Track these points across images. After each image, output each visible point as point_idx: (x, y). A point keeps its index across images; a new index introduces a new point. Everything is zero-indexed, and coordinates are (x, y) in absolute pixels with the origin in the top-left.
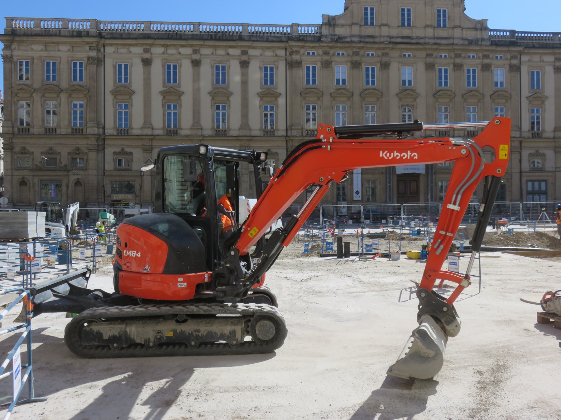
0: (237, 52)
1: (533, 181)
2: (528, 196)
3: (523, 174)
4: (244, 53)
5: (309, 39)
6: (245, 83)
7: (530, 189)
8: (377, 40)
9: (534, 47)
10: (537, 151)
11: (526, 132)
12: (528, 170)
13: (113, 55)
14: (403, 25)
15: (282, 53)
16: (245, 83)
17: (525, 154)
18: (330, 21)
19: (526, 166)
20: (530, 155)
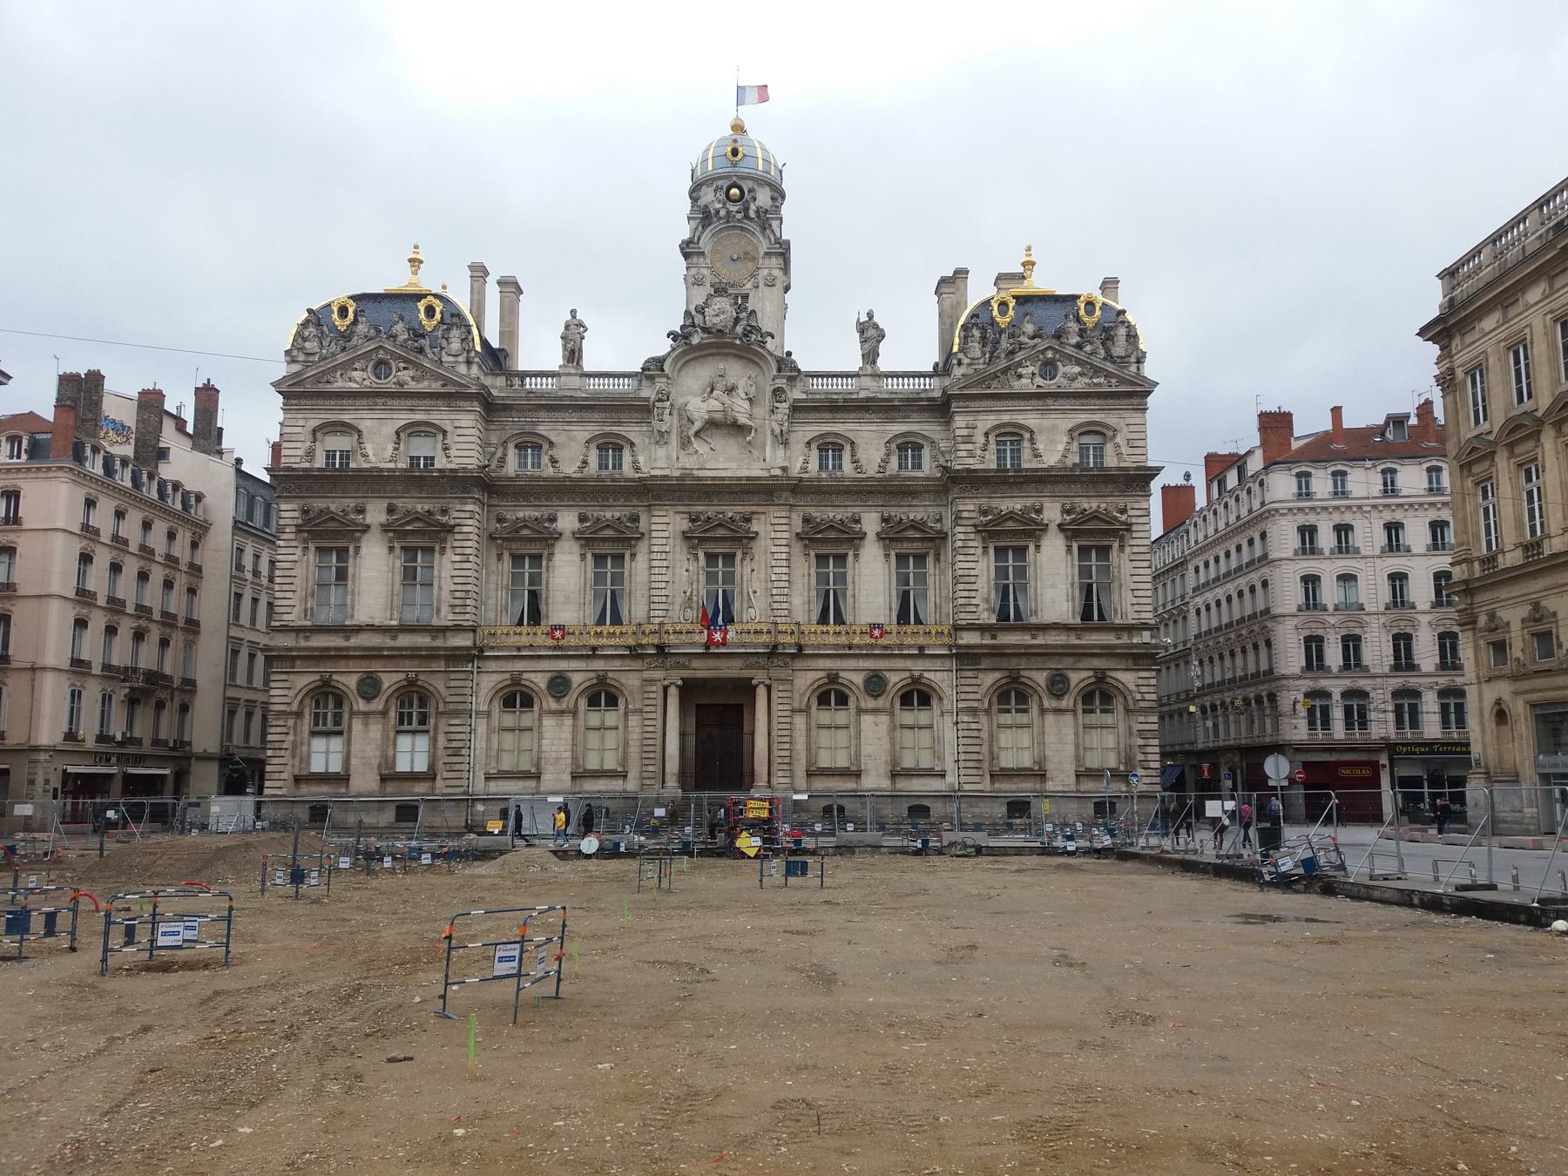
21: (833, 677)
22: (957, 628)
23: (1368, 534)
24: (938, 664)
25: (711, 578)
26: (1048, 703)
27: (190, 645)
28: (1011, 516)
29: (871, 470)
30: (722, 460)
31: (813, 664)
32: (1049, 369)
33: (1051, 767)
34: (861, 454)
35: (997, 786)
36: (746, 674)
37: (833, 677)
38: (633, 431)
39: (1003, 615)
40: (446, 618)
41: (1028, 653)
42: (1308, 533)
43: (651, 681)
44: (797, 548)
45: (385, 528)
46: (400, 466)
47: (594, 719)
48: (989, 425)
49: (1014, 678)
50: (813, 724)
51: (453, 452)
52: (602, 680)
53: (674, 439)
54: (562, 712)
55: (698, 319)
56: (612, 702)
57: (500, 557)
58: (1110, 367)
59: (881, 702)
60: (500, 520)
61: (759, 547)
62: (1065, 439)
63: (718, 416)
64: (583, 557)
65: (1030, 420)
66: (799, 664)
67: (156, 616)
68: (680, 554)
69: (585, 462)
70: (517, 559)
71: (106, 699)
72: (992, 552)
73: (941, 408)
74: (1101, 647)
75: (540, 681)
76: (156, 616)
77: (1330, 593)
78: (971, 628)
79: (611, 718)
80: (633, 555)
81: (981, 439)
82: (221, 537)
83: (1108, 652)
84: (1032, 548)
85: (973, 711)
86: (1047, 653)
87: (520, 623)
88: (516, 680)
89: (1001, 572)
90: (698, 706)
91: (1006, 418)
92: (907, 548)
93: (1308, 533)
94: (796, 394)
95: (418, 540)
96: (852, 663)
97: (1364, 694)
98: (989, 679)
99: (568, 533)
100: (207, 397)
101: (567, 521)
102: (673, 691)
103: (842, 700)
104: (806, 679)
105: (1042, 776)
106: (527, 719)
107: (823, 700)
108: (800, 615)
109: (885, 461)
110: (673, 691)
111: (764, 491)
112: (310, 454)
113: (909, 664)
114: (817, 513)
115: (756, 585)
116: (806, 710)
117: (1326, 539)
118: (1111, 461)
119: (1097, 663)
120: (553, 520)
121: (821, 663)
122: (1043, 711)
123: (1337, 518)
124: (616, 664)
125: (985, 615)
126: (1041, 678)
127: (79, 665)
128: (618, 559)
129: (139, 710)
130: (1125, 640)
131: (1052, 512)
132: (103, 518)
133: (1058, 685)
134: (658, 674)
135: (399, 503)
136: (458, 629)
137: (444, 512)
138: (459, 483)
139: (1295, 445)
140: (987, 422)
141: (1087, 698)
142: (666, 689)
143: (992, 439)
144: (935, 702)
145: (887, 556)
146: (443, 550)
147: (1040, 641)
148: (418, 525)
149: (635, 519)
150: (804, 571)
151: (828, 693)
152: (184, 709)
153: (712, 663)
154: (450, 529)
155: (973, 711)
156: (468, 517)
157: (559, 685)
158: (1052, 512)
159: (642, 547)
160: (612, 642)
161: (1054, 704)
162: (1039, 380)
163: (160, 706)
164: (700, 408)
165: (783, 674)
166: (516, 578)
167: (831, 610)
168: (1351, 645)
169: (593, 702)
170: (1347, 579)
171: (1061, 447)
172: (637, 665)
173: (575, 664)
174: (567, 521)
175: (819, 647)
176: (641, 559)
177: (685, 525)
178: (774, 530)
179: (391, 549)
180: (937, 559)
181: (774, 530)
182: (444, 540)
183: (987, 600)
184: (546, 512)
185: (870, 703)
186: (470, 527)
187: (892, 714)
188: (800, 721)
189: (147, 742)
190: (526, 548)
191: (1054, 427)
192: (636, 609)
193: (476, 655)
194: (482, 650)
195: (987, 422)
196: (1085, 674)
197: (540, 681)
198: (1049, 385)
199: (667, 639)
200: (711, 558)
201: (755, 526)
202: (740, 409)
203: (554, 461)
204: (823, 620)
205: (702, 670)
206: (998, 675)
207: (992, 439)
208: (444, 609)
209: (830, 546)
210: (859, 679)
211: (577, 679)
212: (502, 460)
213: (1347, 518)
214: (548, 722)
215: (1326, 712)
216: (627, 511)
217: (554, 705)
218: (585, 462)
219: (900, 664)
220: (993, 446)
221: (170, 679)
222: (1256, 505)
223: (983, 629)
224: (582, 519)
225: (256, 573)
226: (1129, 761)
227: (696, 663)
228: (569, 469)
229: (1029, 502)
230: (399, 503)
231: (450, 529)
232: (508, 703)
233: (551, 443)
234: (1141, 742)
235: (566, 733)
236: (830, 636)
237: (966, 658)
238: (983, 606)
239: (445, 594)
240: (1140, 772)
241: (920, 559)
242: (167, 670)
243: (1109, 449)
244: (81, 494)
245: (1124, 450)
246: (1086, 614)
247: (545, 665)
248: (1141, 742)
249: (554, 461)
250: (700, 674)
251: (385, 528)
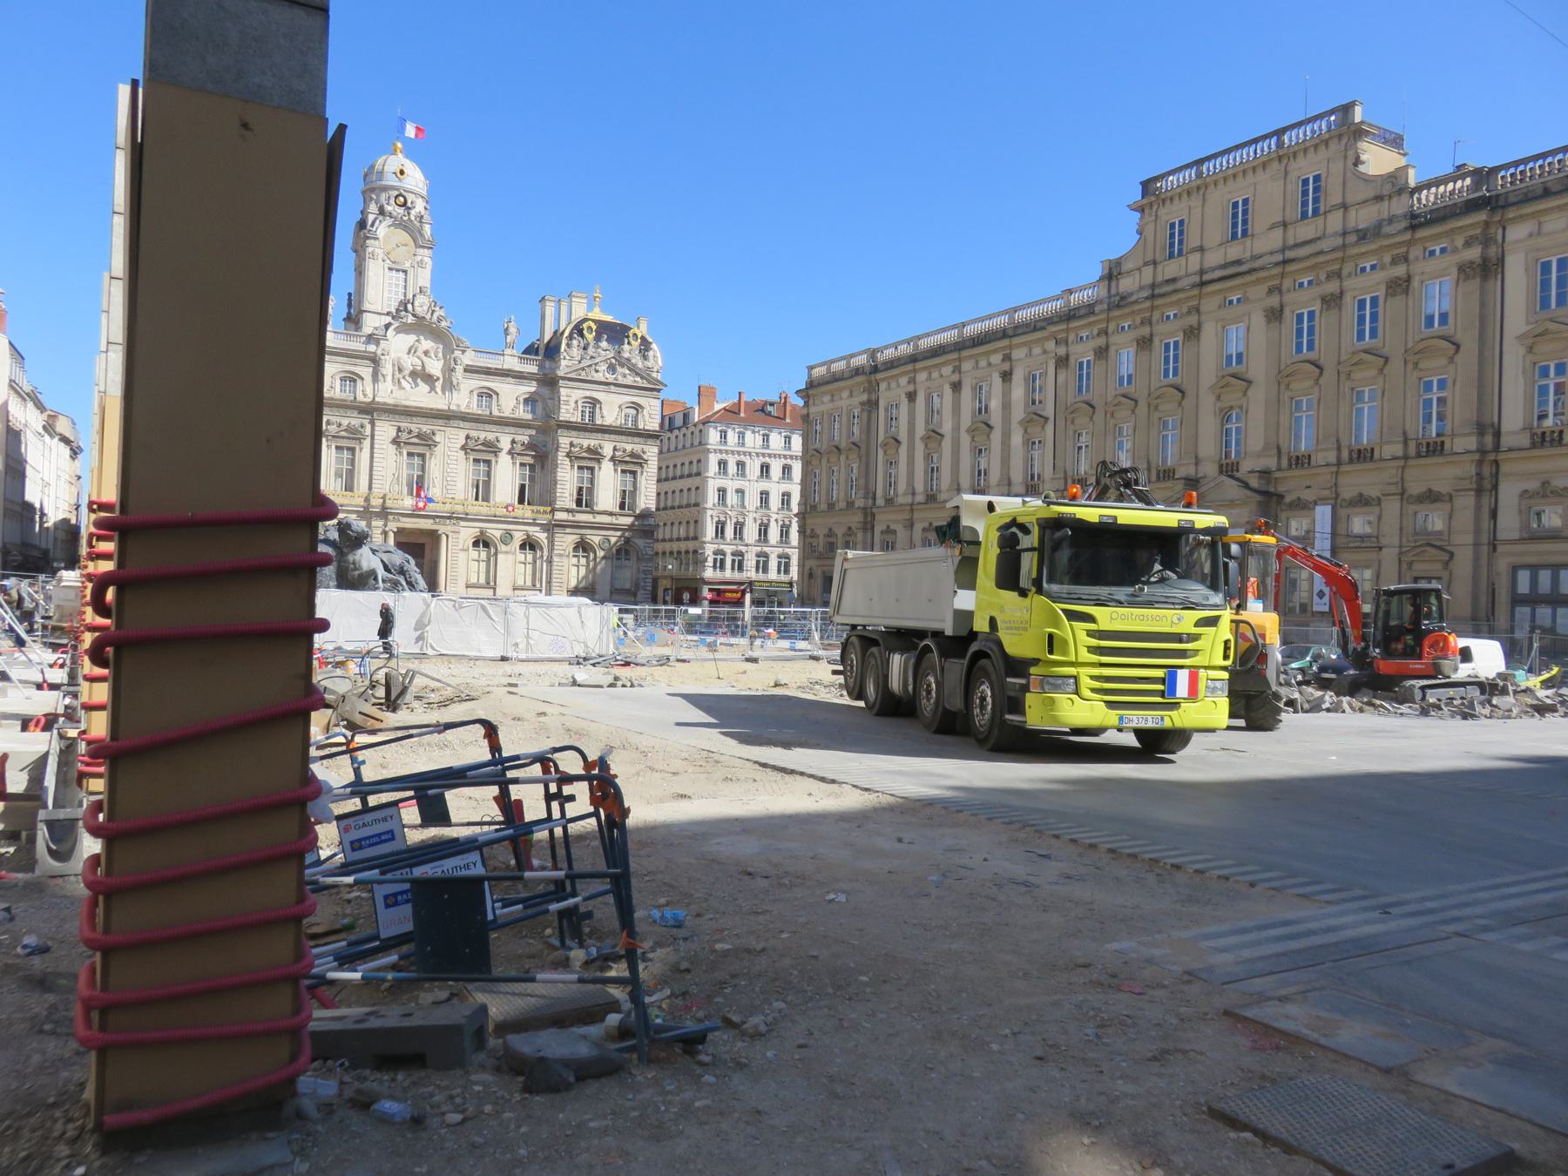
0: (996, 359)
1: (1534, 569)
2: (1518, 609)
3: (1500, 548)
4: (1007, 358)
5: (1082, 312)
6: (1006, 406)
7: (1523, 587)
8: (1179, 285)
9: (1547, 193)
10: (1545, 483)
11: (1514, 433)
12: (1516, 535)
13: (892, 392)
14: (1234, 236)
15: (1051, 345)
16: (1006, 406)
17: (1509, 493)
18: (1112, 273)
19: (1509, 524)
20: (1524, 494)
23: (753, 468)
28: (589, 450)
29: (507, 413)
30: (419, 396)
32: (612, 368)
38: (366, 371)
42: (723, 464)
53: (389, 378)
55: (410, 307)
61: (438, 450)
77: (732, 498)
91: (588, 394)
93: (723, 464)
94: (469, 358)
97: (741, 554)
108: (460, 496)
111: (447, 417)
114: (474, 434)
117: (732, 468)
123: (737, 458)
131: (608, 450)
139: (718, 407)
158: (608, 450)
164: (410, 363)
165: (455, 528)
168: (739, 528)
170: (740, 492)
178: (450, 440)
181: (450, 440)
188: (462, 555)
198: (610, 378)
199: (389, 503)
200: (410, 454)
201: (437, 438)
202: (435, 367)
205: (409, 523)
209: (482, 455)
210: (498, 534)
213: (742, 458)
215: (722, 562)
222: (696, 443)
223: (568, 511)
226: (637, 586)
236: (481, 509)
246: (622, 506)
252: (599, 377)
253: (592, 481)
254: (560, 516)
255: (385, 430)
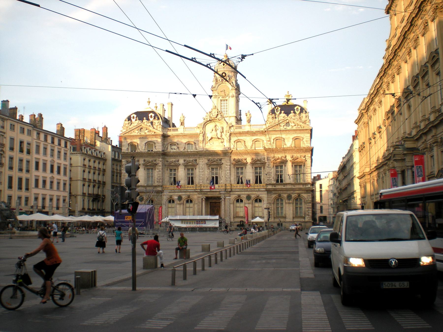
21: (239, 196)
22: (267, 185)
24: (263, 192)
25: (213, 173)
26: (287, 201)
27: (104, 187)
31: (234, 193)
33: (287, 216)
34: (247, 144)
35: (275, 220)
36: (219, 196)
37: (239, 196)
39: (277, 181)
40: (156, 184)
41: (282, 190)
43: (199, 197)
44: (232, 166)
45: (143, 165)
46: (146, 151)
47: (188, 205)
48: (274, 137)
49: (280, 195)
50: (235, 206)
51: (157, 148)
52: (189, 197)
54: (180, 204)
56: (191, 201)
57: (167, 170)
58: (301, 124)
59: (250, 201)
60: (167, 161)
61: (223, 166)
62: (292, 140)
63: (213, 136)
64: (185, 169)
65: (284, 136)
66: (231, 193)
67: (97, 182)
68: (206, 167)
69: (185, 148)
70: (171, 170)
71: (89, 201)
72: (275, 167)
73: (263, 133)
74: (299, 188)
75: (175, 198)
76: (97, 182)
78: (270, 184)
79: (191, 205)
80: (196, 169)
81: (272, 141)
82: (109, 162)
83: (300, 189)
84: (284, 166)
85: (270, 203)
86: (287, 190)
87: (172, 184)
88: (171, 197)
89: (277, 172)
90: (210, 203)
92: (257, 166)
95: (150, 167)
96: (243, 193)
98: (274, 196)
99: (181, 164)
100: (105, 129)
101: (181, 161)
102: (203, 199)
103: (242, 201)
104: (233, 196)
105: (285, 217)
106: (173, 205)
107: (237, 201)
109: (252, 145)
110: (203, 199)
112: (128, 149)
113: (256, 193)
115: (223, 175)
116: (234, 203)
118: (302, 145)
119: (297, 192)
120: (178, 161)
121: (237, 193)
122: (286, 203)
124: (192, 193)
125: (273, 182)
126: (285, 196)
127: (84, 194)
128: (192, 169)
129: (94, 202)
130: (304, 187)
132: (87, 162)
133: (289, 197)
134: (200, 196)
135: (146, 159)
136: (159, 186)
137: (155, 161)
138: (157, 154)
140: (273, 137)
141: (296, 200)
142: (202, 199)
143: (275, 140)
144: (262, 201)
145: (253, 168)
146: (155, 169)
147: (285, 187)
148: (150, 164)
149: (196, 160)
150: (233, 171)
151: (238, 199)
152: (103, 201)
153: (212, 193)
154: (156, 164)
155: (270, 203)
156: (159, 161)
157: (180, 198)
158: (289, 158)
159: (197, 167)
160: (190, 189)
161: (288, 201)
162: (285, 127)
163: (98, 201)
166: (171, 174)
167: (239, 181)
169: (187, 201)
171: (290, 142)
172: (196, 193)
173: (183, 193)
174: (181, 161)
175: (236, 189)
176: (197, 170)
177: (207, 161)
179: (145, 169)
180: (264, 168)
182: (155, 167)
183: (274, 178)
184: (177, 159)
185: (248, 202)
186: (160, 164)
187: (252, 204)
189: (96, 209)
190: (173, 168)
191: (289, 138)
192: (196, 181)
193: (162, 192)
194: (163, 190)
195: (273, 137)
196: (296, 195)
197: (175, 198)
200: (213, 169)
201: (223, 162)
203: (178, 148)
204: (238, 183)
205: (210, 195)
206: (276, 195)
207: (275, 140)
208: (156, 182)
210: (245, 196)
211: (183, 197)
212: (167, 148)
214: (178, 206)
216: (194, 159)
217: (179, 202)
218: (185, 148)
219: (254, 193)
220: (275, 142)
221: (100, 195)
224: (185, 161)
225: (117, 169)
227: (208, 193)
228: (182, 150)
229: (284, 155)
230: (146, 159)
231: (156, 164)
232: (170, 202)
233: (178, 144)
234: (307, 210)
235: (182, 209)
237: (269, 191)
238: (273, 179)
239: (156, 179)
240: (307, 216)
241: (260, 168)
242: (99, 193)
243: (302, 142)
244: (83, 157)
245: (305, 143)
247: (176, 194)
248: (307, 210)
249: (178, 148)
250: (210, 196)
251: (143, 165)
252: (282, 128)
253: (281, 171)
254: (270, 187)
255: (202, 162)
